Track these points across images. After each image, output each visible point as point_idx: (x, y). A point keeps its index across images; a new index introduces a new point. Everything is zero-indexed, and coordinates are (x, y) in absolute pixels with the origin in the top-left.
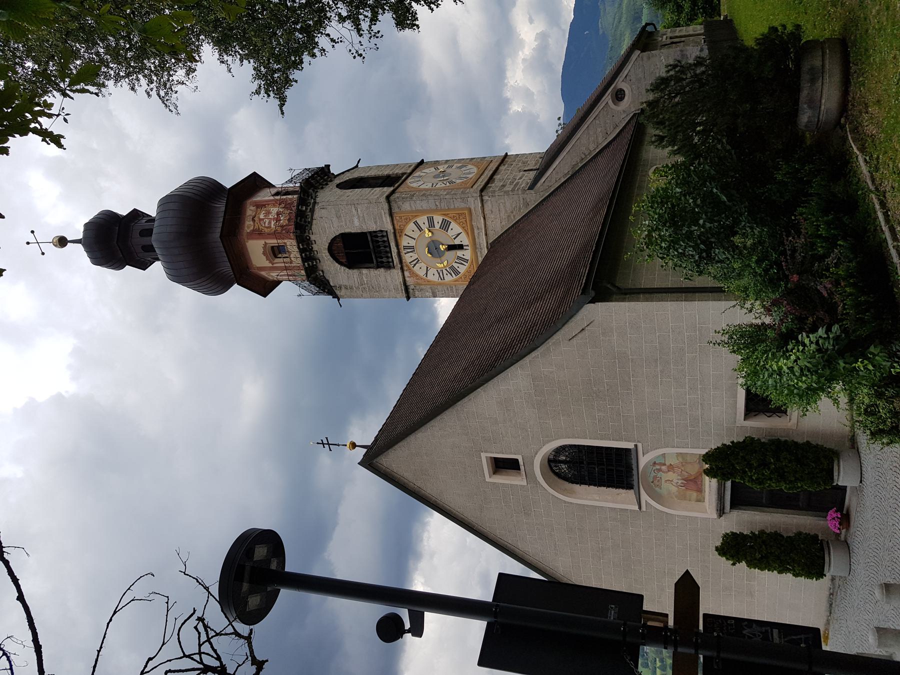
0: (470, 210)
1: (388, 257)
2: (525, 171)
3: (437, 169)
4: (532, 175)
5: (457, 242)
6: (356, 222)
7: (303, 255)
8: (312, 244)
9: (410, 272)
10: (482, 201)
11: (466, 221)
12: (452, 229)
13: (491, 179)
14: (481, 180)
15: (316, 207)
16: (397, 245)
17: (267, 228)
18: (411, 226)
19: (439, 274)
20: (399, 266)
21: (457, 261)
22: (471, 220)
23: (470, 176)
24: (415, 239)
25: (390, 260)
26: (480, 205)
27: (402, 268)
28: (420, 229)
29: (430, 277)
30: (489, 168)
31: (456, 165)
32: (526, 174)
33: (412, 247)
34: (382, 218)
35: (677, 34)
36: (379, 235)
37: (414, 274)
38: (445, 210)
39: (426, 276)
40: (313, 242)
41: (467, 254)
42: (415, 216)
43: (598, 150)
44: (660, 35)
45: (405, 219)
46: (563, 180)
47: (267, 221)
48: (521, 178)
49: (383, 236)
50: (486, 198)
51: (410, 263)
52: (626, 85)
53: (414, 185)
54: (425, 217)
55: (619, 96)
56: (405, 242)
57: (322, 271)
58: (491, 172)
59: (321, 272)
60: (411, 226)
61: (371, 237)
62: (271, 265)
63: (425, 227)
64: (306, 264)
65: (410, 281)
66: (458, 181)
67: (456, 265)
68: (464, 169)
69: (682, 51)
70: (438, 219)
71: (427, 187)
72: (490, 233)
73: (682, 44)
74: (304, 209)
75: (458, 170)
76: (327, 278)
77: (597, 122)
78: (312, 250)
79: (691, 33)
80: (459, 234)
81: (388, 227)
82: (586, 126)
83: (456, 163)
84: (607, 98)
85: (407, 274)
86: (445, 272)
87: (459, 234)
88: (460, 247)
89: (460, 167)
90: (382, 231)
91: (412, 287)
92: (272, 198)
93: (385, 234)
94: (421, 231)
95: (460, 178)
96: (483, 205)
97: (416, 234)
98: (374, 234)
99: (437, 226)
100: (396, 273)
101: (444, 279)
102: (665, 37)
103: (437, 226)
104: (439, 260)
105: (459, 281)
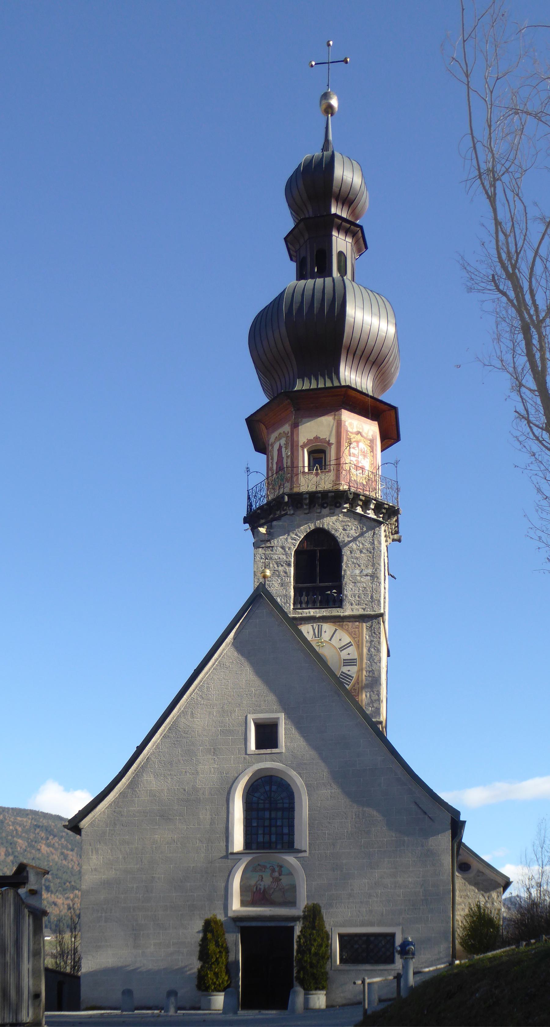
1: (307, 603)
7: (320, 495)
8: (330, 509)
16: (324, 619)
18: (347, 639)
24: (330, 640)
25: (304, 606)
28: (343, 648)
40: (332, 511)
45: (355, 631)
57: (293, 514)
76: (283, 518)
78: (323, 507)
81: (347, 611)
94: (339, 649)
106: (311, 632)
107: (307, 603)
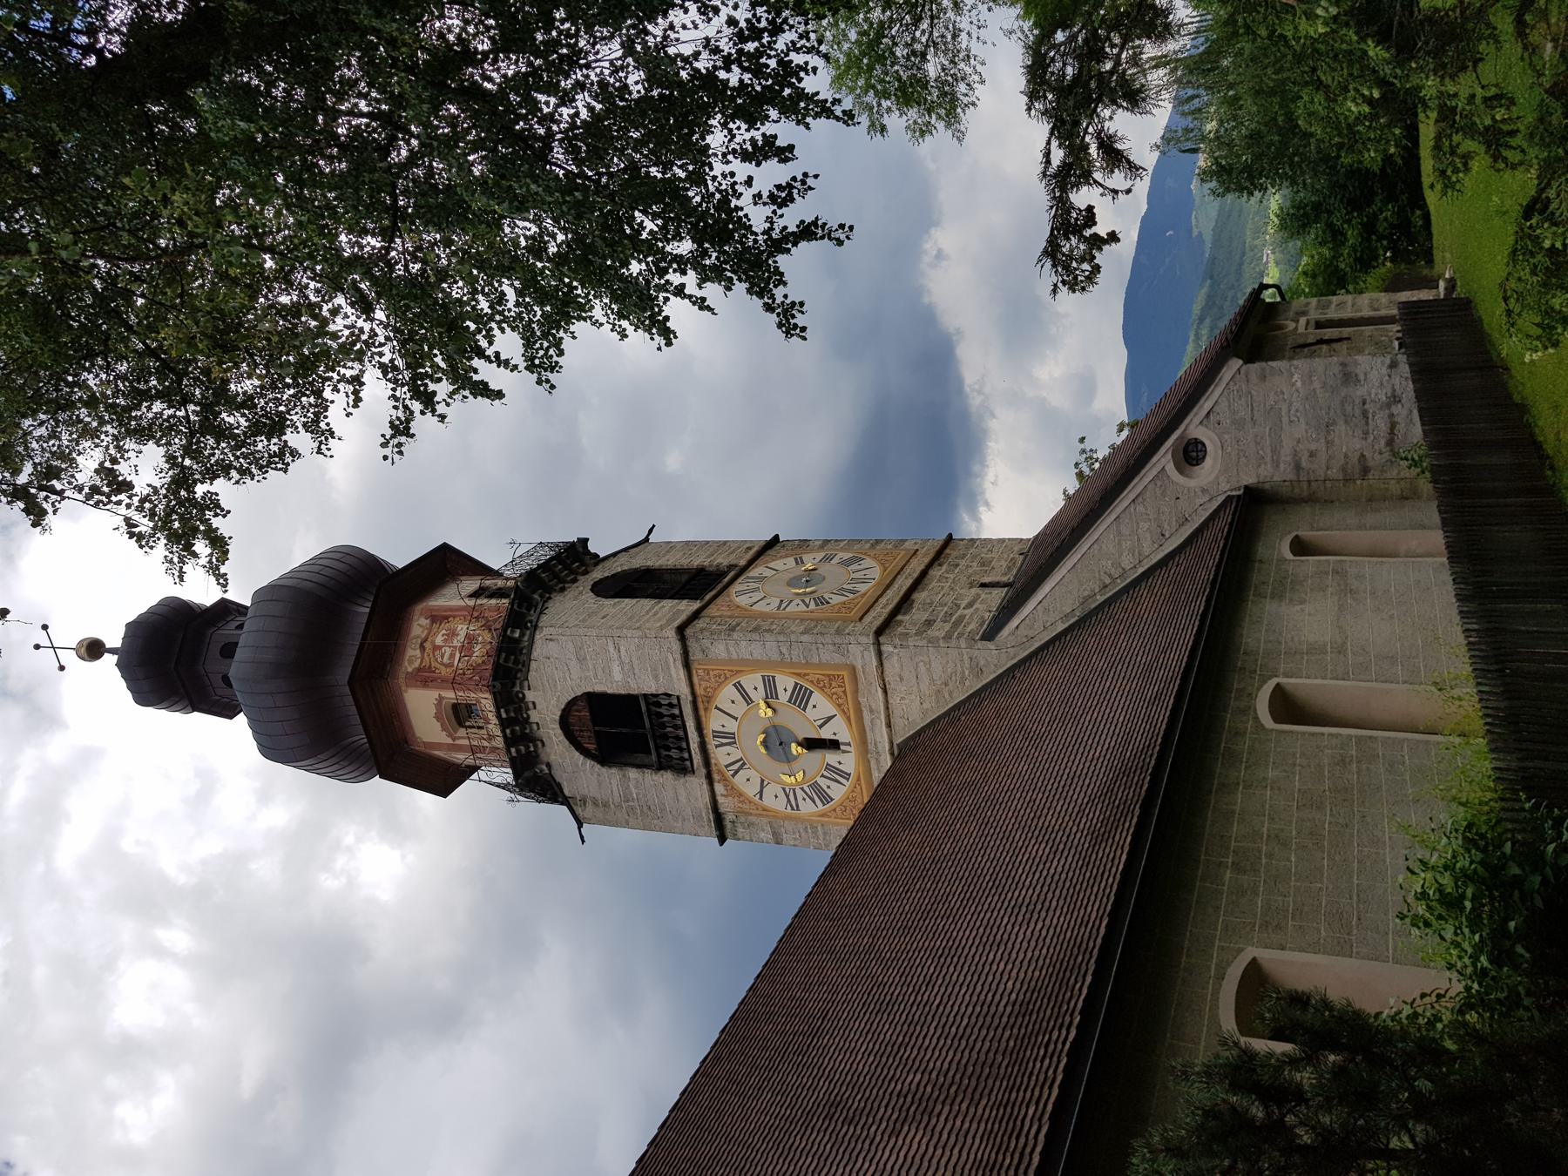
0: (853, 670)
2: (983, 585)
3: (799, 562)
4: (996, 597)
5: (826, 734)
6: (617, 675)
7: (508, 731)
9: (726, 786)
10: (879, 654)
11: (844, 692)
13: (905, 602)
14: (883, 600)
15: (537, 637)
16: (700, 728)
17: (446, 666)
18: (729, 691)
19: (787, 796)
20: (704, 771)
21: (826, 774)
22: (856, 691)
23: (863, 588)
24: (736, 719)
25: (686, 755)
26: (875, 663)
27: (709, 778)
28: (748, 699)
29: (768, 801)
30: (908, 570)
31: (840, 555)
32: (984, 593)
33: (732, 736)
34: (668, 668)
35: (1332, 314)
36: (663, 702)
37: (733, 791)
38: (798, 665)
40: (531, 705)
41: (847, 761)
42: (737, 672)
43: (1140, 570)
44: (1291, 314)
45: (715, 676)
46: (1061, 627)
47: (448, 651)
48: (970, 605)
49: (671, 705)
50: (886, 648)
51: (727, 766)
52: (1210, 433)
53: (743, 601)
54: (758, 676)
55: (1191, 454)
56: (714, 722)
57: (548, 765)
58: (909, 582)
59: (544, 767)
60: (729, 691)
61: (648, 704)
62: (450, 741)
63: (758, 696)
64: (513, 750)
65: (726, 804)
66: (836, 599)
67: (823, 783)
68: (855, 567)
69: (1343, 365)
70: (785, 683)
71: (767, 609)
72: (898, 722)
73: (1344, 345)
74: (517, 635)
75: (842, 570)
76: (558, 779)
77: (1140, 508)
78: (527, 720)
79: (1366, 313)
80: (830, 718)
81: (681, 689)
82: (1113, 516)
83: (842, 550)
84: (1163, 459)
85: (719, 788)
86: (800, 793)
87: (830, 718)
88: (834, 745)
89: (846, 563)
90: (669, 695)
91: (729, 817)
92: (471, 602)
93: (675, 701)
95: (841, 591)
96: (881, 663)
97: (740, 708)
98: (652, 700)
99: (784, 697)
100: (697, 783)
101: (798, 809)
102: (1303, 321)
103: (784, 697)
104: (785, 767)
106: (728, 748)
107: (681, 749)
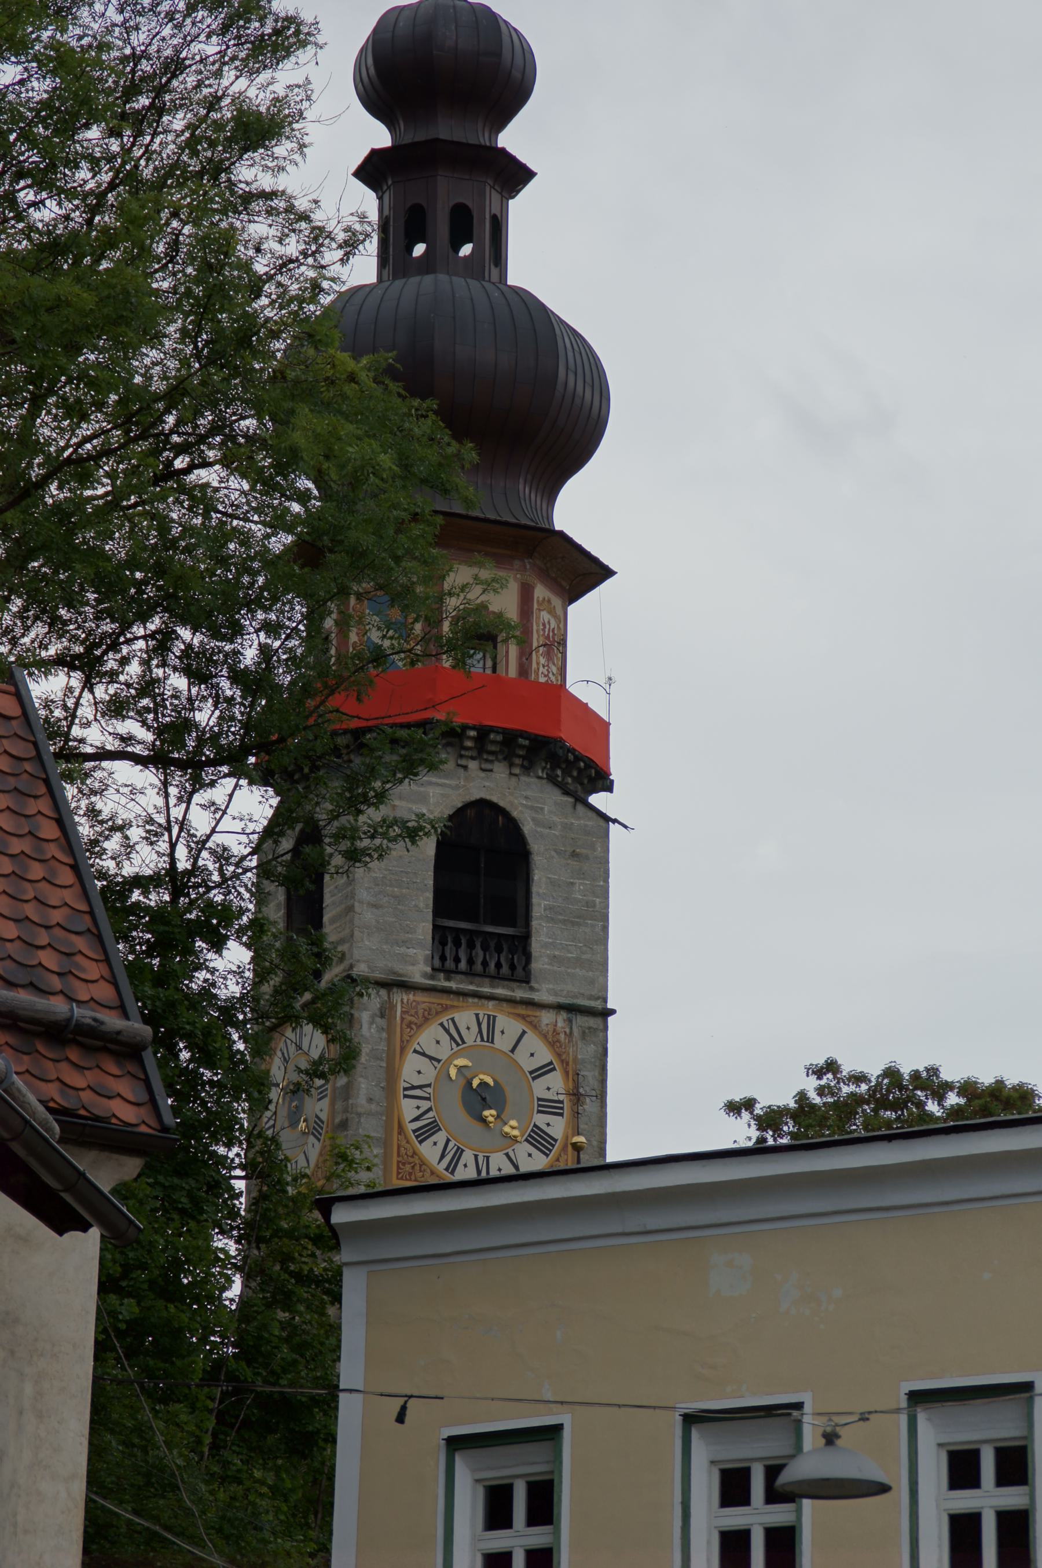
12: (530, 1155)
19: (420, 1087)
24: (513, 1051)
39: (415, 1051)
51: (453, 1019)
56: (508, 1025)
60: (545, 1055)
86: (425, 1105)
99: (541, 1120)
103: (541, 1120)
105: (399, 1133)
106: (475, 1028)
